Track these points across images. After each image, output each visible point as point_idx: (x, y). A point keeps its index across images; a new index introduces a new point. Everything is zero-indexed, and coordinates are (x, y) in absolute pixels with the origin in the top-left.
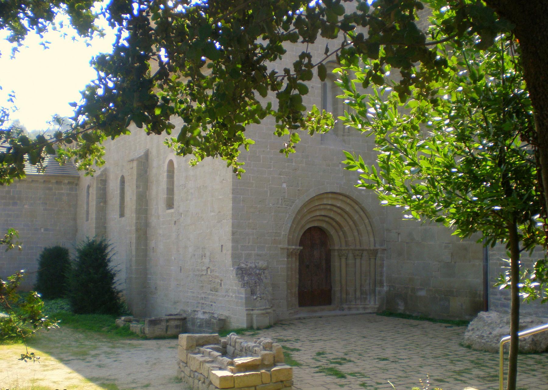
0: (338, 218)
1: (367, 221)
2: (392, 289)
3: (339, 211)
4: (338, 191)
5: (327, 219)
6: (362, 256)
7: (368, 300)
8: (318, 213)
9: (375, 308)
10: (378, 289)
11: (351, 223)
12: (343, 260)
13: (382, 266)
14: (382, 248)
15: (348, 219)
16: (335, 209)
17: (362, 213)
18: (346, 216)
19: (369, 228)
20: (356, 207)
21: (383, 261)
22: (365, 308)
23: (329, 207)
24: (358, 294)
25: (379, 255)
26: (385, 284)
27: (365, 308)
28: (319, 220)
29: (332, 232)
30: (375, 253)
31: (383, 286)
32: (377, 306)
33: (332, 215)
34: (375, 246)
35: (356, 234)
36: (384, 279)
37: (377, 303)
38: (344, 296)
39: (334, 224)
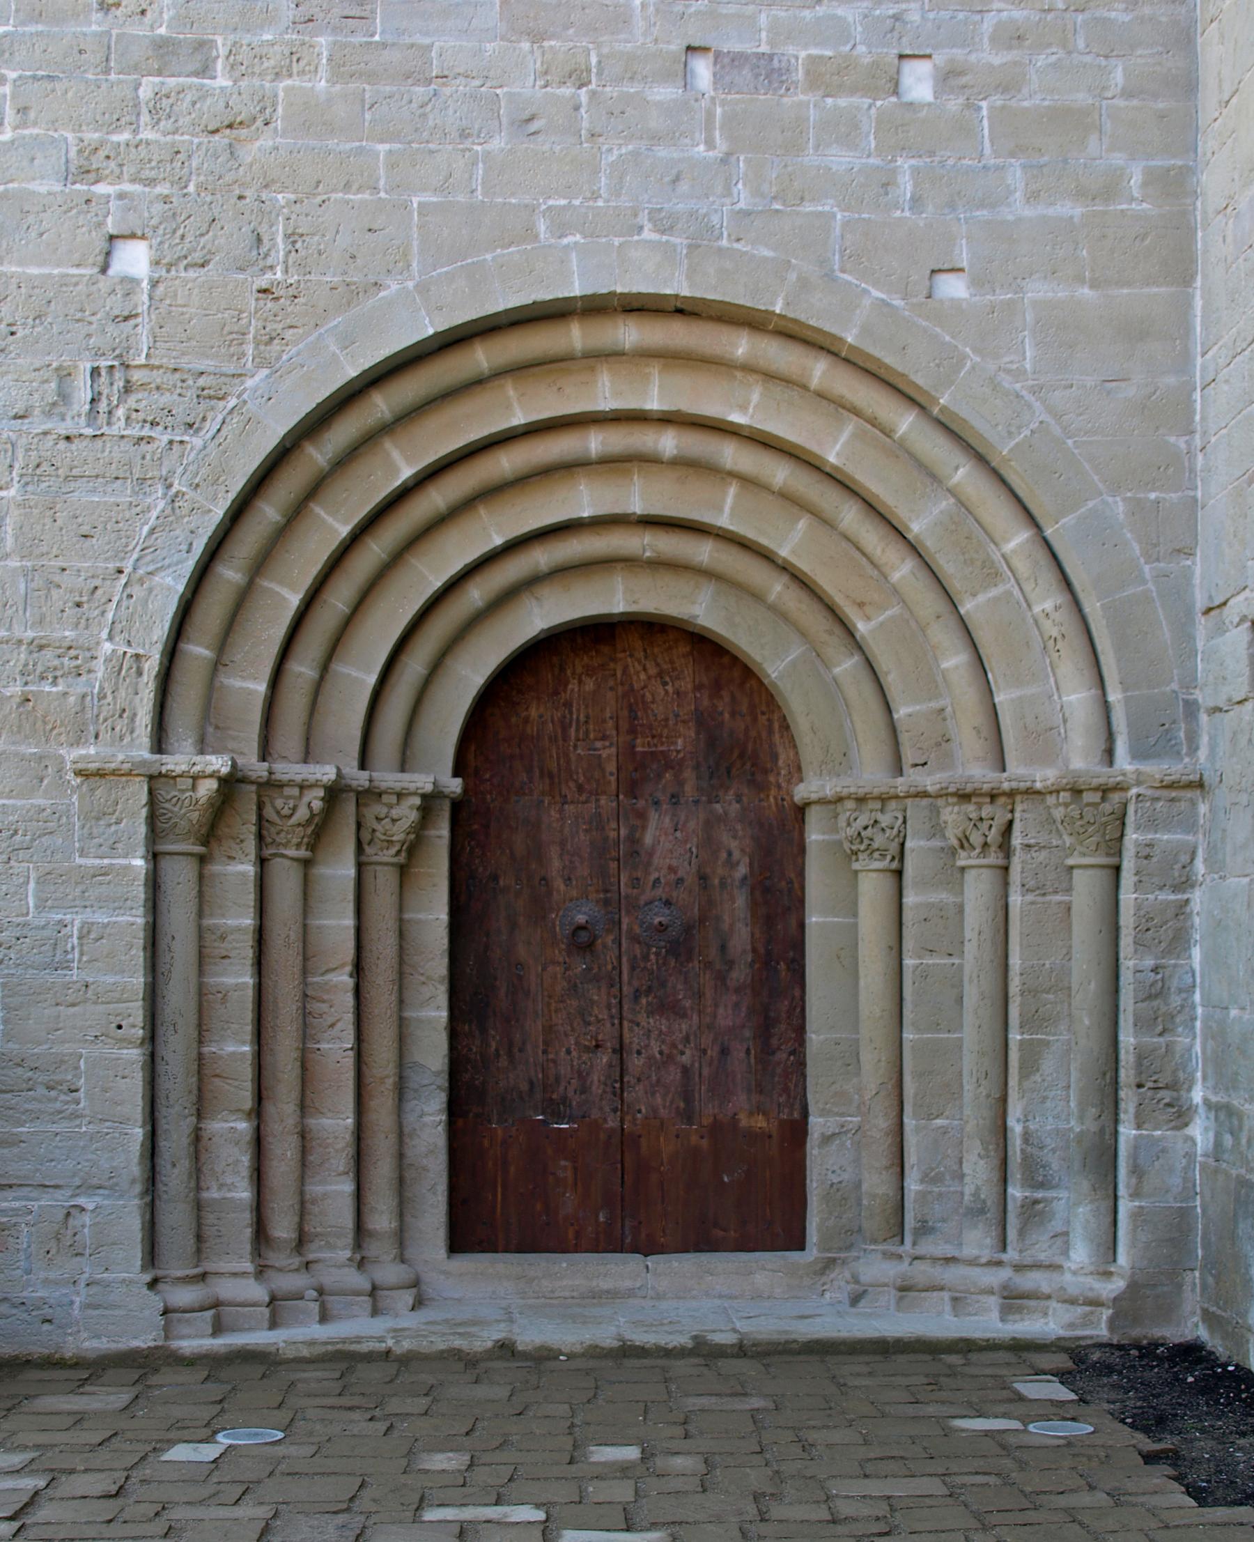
0: (791, 540)
1: (1018, 540)
2: (1228, 1140)
3: (780, 473)
4: (678, 286)
5: (703, 552)
6: (1005, 846)
7: (1057, 1225)
8: (584, 499)
9: (1096, 1303)
10: (1127, 1132)
11: (903, 570)
12: (872, 887)
13: (1170, 932)
14: (1156, 769)
15: (871, 537)
16: (730, 454)
17: (963, 473)
18: (850, 516)
19: (1048, 602)
20: (906, 422)
21: (1186, 883)
22: (1013, 1300)
23: (668, 442)
24: (977, 1171)
25: (1132, 837)
26: (1197, 1095)
27: (1013, 1300)
28: (628, 562)
29: (777, 662)
30: (1101, 813)
31: (1181, 1116)
32: (1117, 1285)
33: (726, 510)
34: (1109, 753)
35: (955, 661)
36: (1194, 1045)
37: (1123, 1259)
38: (877, 1184)
39: (777, 588)
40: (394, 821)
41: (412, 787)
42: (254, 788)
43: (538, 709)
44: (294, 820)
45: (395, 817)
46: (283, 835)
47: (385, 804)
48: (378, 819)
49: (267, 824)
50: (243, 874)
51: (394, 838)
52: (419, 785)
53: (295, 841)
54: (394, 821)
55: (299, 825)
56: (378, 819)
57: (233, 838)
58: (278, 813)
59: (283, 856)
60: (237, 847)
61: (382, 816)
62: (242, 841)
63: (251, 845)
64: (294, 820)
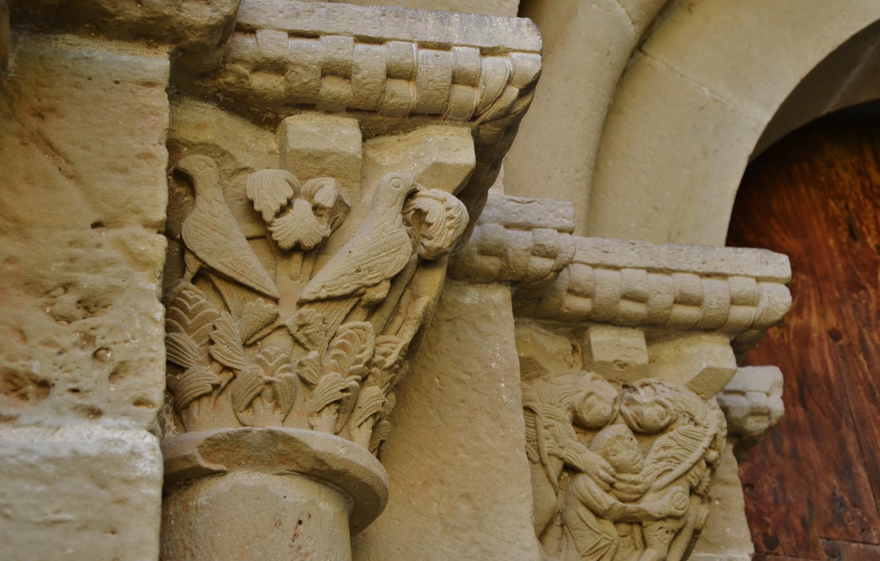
40: (645, 432)
41: (715, 294)
42: (157, 62)
43: (823, 315)
44: (332, 274)
45: (652, 414)
46: (277, 344)
47: (603, 369)
48: (585, 427)
49: (198, 297)
50: (100, 470)
51: (652, 504)
52: (742, 286)
53: (331, 384)
54: (645, 432)
55: (358, 301)
56: (585, 427)
57: (35, 286)
58: (262, 232)
59: (283, 454)
60: (68, 335)
61: (600, 408)
62: (90, 305)
63: (139, 326)
64: (332, 274)
